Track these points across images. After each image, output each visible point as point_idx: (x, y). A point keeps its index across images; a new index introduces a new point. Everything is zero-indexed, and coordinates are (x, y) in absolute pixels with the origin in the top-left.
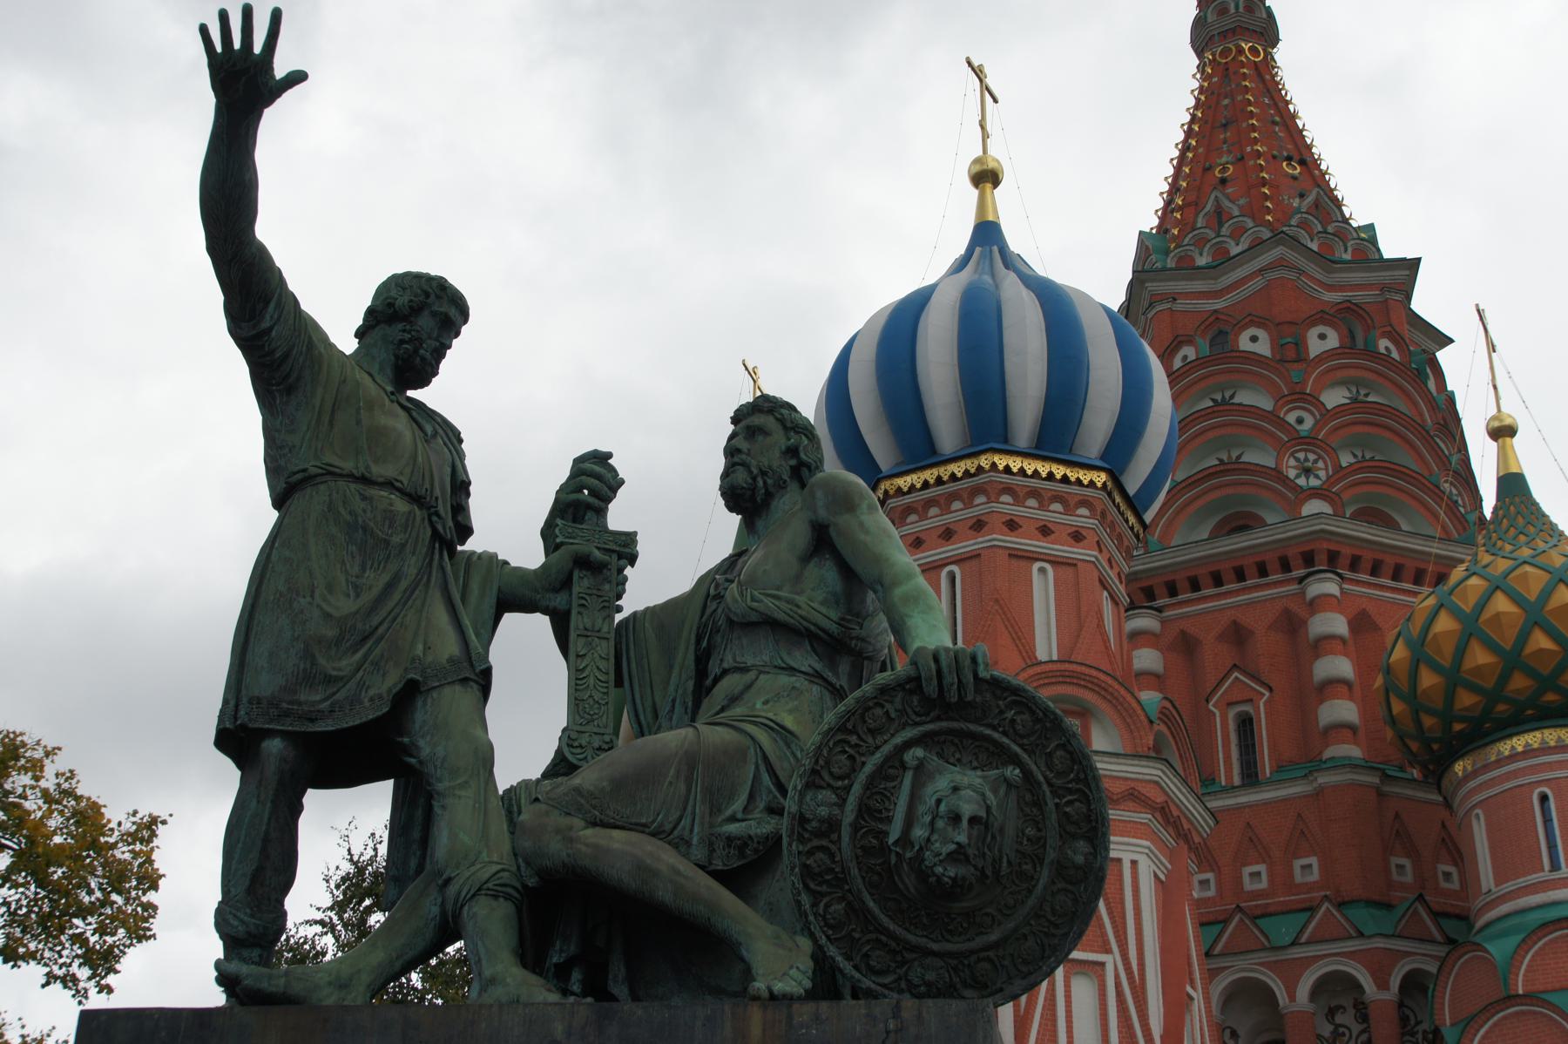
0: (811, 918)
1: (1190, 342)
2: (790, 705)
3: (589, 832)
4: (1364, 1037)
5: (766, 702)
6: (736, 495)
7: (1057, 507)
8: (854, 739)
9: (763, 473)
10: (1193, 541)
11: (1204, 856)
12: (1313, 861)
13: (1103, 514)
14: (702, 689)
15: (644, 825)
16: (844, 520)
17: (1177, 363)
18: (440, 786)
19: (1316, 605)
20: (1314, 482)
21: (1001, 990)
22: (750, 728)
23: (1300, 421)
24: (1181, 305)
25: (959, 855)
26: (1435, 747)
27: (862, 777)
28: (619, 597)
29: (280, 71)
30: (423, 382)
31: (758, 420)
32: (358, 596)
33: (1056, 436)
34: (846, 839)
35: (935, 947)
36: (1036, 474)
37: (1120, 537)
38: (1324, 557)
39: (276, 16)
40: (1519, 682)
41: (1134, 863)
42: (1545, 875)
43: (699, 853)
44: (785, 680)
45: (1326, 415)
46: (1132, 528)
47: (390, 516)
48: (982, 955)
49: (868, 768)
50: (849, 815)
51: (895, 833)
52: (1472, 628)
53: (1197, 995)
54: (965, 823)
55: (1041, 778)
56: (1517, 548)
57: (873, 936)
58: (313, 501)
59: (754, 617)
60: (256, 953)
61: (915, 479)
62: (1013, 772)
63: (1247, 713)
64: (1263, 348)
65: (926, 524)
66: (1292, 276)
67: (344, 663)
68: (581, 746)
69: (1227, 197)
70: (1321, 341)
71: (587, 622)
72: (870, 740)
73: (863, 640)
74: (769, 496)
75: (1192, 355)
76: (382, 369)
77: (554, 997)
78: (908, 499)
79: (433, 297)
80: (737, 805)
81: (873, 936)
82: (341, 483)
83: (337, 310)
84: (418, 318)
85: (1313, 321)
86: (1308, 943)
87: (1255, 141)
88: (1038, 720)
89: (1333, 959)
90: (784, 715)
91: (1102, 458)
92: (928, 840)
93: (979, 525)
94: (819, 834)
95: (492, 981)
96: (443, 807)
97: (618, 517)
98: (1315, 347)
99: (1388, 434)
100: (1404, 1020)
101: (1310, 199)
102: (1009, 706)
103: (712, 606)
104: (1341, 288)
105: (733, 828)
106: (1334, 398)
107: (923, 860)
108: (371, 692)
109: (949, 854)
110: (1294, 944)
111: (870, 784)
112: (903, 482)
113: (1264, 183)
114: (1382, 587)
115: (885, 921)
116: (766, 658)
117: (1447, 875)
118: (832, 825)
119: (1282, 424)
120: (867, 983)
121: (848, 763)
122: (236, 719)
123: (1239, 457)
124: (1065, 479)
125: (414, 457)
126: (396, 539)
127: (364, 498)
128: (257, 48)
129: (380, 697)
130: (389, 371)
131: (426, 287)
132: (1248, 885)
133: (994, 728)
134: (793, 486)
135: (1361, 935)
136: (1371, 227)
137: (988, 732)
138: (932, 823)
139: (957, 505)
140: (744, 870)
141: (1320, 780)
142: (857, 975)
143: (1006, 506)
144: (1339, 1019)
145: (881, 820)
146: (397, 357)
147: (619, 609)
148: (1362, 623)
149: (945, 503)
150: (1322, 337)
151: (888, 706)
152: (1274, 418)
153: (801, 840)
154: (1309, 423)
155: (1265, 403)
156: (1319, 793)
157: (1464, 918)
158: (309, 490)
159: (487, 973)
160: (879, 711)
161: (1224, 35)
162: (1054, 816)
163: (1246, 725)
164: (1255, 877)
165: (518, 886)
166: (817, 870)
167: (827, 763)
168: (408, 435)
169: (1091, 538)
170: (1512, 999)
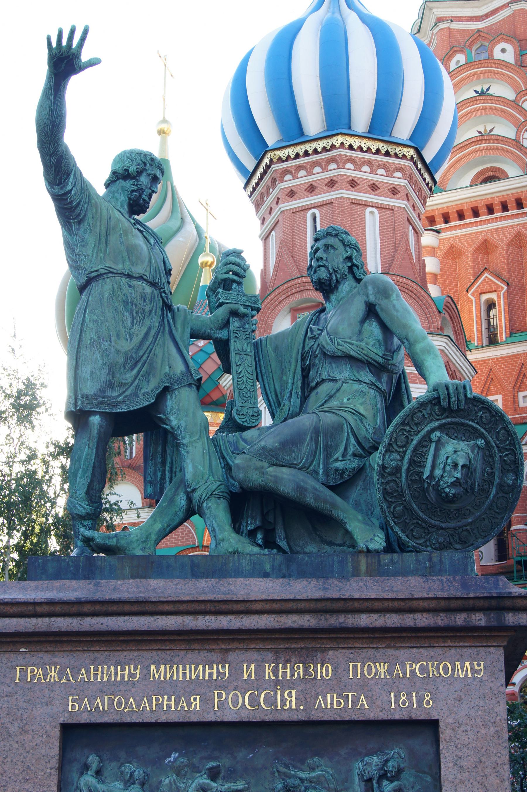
0: (387, 514)
1: (461, 51)
2: (361, 401)
3: (271, 469)
5: (348, 399)
7: (381, 171)
8: (408, 428)
9: (335, 271)
13: (411, 176)
15: (296, 464)
16: (384, 303)
17: (453, 66)
18: (185, 441)
21: (472, 544)
25: (457, 483)
31: (331, 241)
32: (131, 340)
33: (381, 124)
34: (404, 476)
35: (443, 525)
37: (420, 190)
39: (86, 32)
44: (356, 386)
46: (427, 185)
47: (143, 296)
48: (465, 528)
49: (414, 443)
50: (405, 467)
51: (426, 473)
54: (460, 467)
55: (494, 444)
57: (415, 521)
58: (104, 287)
59: (339, 354)
60: (90, 522)
61: (291, 152)
62: (481, 442)
63: (493, 300)
64: (510, 57)
67: (128, 375)
68: (243, 414)
71: (239, 346)
72: (416, 428)
73: (394, 365)
74: (338, 282)
76: (122, 206)
77: (256, 549)
78: (285, 165)
79: (148, 165)
80: (338, 454)
81: (415, 521)
82: (118, 278)
88: (493, 416)
90: (359, 406)
91: (410, 139)
92: (442, 476)
93: (332, 183)
94: (391, 474)
95: (223, 540)
96: (188, 452)
103: (310, 343)
105: (337, 465)
107: (439, 485)
108: (143, 391)
109: (452, 483)
111: (415, 450)
115: (421, 513)
116: (347, 375)
118: (397, 470)
120: (412, 543)
121: (405, 439)
123: (491, 131)
126: (147, 309)
127: (130, 286)
128: (74, 46)
129: (148, 393)
130: (126, 207)
131: (144, 160)
133: (473, 421)
134: (350, 277)
137: (470, 423)
138: (444, 468)
139: (317, 169)
140: (342, 485)
142: (408, 540)
145: (420, 467)
146: (130, 199)
149: (309, 169)
151: (424, 412)
153: (383, 477)
155: (510, 95)
158: (100, 282)
159: (220, 536)
160: (420, 414)
162: (499, 462)
165: (228, 491)
166: (390, 491)
167: (396, 440)
168: (145, 247)
169: (402, 193)
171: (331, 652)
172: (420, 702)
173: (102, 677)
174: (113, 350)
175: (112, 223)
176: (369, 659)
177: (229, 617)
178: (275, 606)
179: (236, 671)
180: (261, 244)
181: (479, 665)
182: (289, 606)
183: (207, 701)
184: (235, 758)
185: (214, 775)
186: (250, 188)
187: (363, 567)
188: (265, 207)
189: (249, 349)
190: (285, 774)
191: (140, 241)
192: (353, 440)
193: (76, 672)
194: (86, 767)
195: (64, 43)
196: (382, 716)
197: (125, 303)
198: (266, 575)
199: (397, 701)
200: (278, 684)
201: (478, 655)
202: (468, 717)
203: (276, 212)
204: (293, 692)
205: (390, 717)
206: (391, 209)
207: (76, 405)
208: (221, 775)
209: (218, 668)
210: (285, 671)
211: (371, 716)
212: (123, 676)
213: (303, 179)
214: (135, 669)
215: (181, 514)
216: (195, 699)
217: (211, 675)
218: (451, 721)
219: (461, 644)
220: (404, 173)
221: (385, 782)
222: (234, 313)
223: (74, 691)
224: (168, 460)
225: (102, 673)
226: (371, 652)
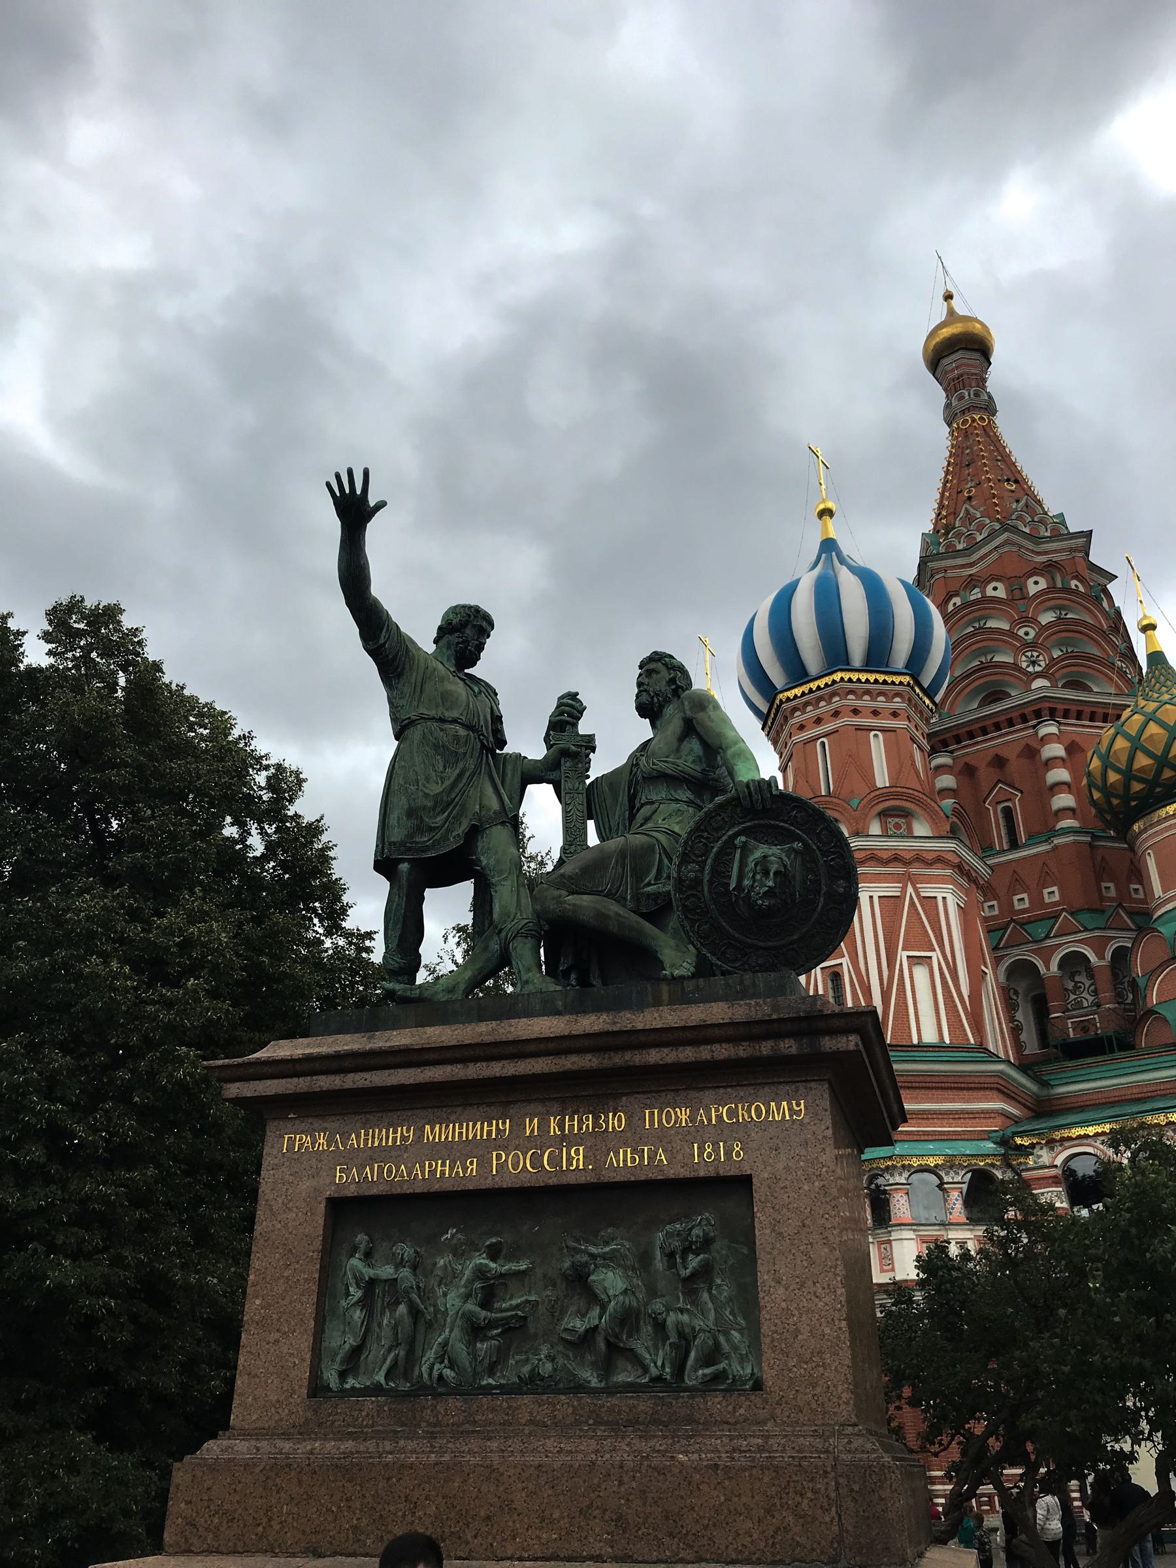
1: (957, 595)
4: (1092, 988)
6: (644, 710)
8: (705, 834)
9: (657, 695)
10: (970, 710)
11: (988, 890)
12: (1055, 889)
14: (632, 817)
15: (602, 891)
17: (950, 608)
19: (1045, 740)
20: (1038, 669)
22: (654, 834)
23: (1027, 634)
24: (950, 574)
25: (770, 893)
28: (588, 770)
29: (372, 503)
30: (473, 664)
31: (652, 666)
35: (762, 944)
36: (867, 681)
37: (921, 712)
38: (1047, 712)
39: (366, 473)
41: (944, 898)
43: (629, 904)
44: (674, 806)
47: (457, 738)
49: (715, 850)
50: (706, 878)
51: (733, 885)
53: (989, 971)
56: (1161, 694)
58: (415, 734)
59: (655, 774)
60: (406, 978)
61: (797, 691)
62: (798, 845)
66: (1015, 549)
70: (1035, 586)
73: (716, 780)
74: (661, 707)
75: (959, 603)
76: (449, 660)
78: (793, 703)
80: (651, 877)
83: (421, 628)
84: (467, 630)
86: (1055, 937)
87: (987, 472)
89: (1071, 945)
91: (906, 667)
93: (836, 714)
95: (527, 982)
97: (584, 728)
98: (1032, 589)
99: (1079, 636)
100: (1115, 975)
101: (1023, 502)
102: (793, 808)
103: (635, 770)
104: (1046, 553)
106: (1046, 618)
110: (1047, 937)
111: (717, 858)
112: (791, 694)
113: (994, 496)
114: (1084, 726)
117: (1136, 890)
118: (697, 882)
122: (383, 854)
125: (468, 705)
126: (461, 750)
127: (442, 730)
128: (359, 492)
132: (1017, 906)
135: (1086, 930)
138: (754, 876)
139: (823, 703)
141: (1055, 842)
144: (1077, 979)
145: (725, 877)
147: (588, 777)
148: (1073, 748)
150: (1036, 583)
152: (1011, 634)
153: (681, 892)
154: (1032, 634)
155: (1005, 626)
156: (1056, 848)
157: (1148, 914)
159: (524, 978)
160: (719, 818)
161: (963, 412)
163: (1008, 814)
164: (1021, 901)
168: (464, 693)
169: (903, 715)
171: (624, 1099)
172: (728, 1153)
173: (373, 1142)
174: (421, 794)
175: (429, 671)
176: (668, 1105)
177: (503, 1062)
178: (551, 1046)
179: (518, 1126)
181: (798, 1105)
183: (484, 1164)
185: (494, 1253)
186: (767, 729)
187: (665, 997)
190: (574, 1248)
193: (345, 1137)
194: (355, 1249)
196: (684, 1173)
198: (558, 1013)
199: (700, 1155)
200: (567, 1140)
201: (796, 1092)
202: (787, 1168)
204: (581, 1149)
208: (504, 1252)
209: (497, 1125)
210: (572, 1124)
211: (671, 1174)
212: (395, 1139)
214: (408, 1131)
216: (472, 1163)
217: (489, 1133)
218: (766, 1175)
219: (776, 1080)
221: (691, 1257)
223: (342, 1160)
225: (373, 1138)
226: (670, 1096)
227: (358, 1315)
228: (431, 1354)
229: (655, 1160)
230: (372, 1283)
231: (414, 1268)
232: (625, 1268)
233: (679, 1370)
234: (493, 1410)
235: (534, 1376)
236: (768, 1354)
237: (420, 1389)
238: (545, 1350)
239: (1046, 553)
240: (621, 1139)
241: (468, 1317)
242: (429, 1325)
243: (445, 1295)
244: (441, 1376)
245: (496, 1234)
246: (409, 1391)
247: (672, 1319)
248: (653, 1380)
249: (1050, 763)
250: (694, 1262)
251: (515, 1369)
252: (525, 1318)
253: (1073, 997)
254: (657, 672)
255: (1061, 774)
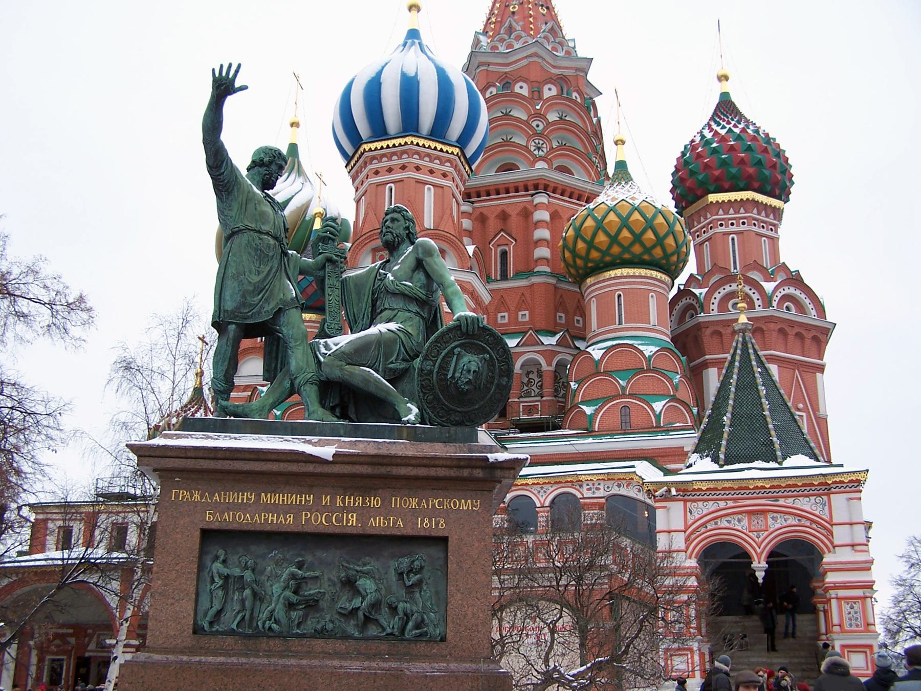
7: (437, 161)
12: (527, 313)
16: (428, 259)
19: (537, 207)
20: (541, 153)
23: (538, 126)
24: (491, 68)
25: (469, 382)
26: (581, 272)
27: (441, 357)
31: (395, 215)
33: (439, 131)
36: (429, 147)
40: (616, 250)
42: (616, 326)
44: (407, 314)
45: (549, 124)
47: (269, 246)
49: (443, 354)
52: (600, 225)
59: (397, 292)
61: (378, 145)
65: (381, 165)
69: (515, 21)
70: (550, 91)
74: (399, 244)
80: (393, 358)
83: (241, 159)
85: (547, 82)
91: (457, 142)
93: (403, 168)
94: (426, 375)
98: (547, 94)
100: (556, 377)
101: (549, 25)
103: (378, 283)
104: (559, 68)
105: (392, 366)
106: (552, 117)
113: (531, 16)
114: (564, 201)
117: (578, 321)
118: (431, 372)
119: (530, 127)
124: (441, 150)
126: (271, 254)
128: (230, 76)
132: (500, 321)
134: (407, 241)
136: (574, 40)
139: (395, 157)
143: (416, 160)
144: (531, 376)
148: (555, 215)
150: (550, 89)
152: (527, 123)
153: (421, 376)
155: (525, 117)
163: (504, 254)
169: (450, 177)
170: (598, 373)
171: (380, 491)
172: (437, 524)
179: (318, 499)
180: (354, 204)
182: (354, 459)
183: (297, 517)
184: (314, 556)
186: (349, 167)
188: (358, 181)
189: (338, 284)
191: (268, 209)
192: (403, 349)
193: (212, 495)
194: (216, 558)
195: (224, 74)
197: (256, 250)
203: (366, 184)
205: (417, 534)
206: (442, 187)
207: (219, 317)
212: (243, 499)
213: (385, 163)
215: (287, 392)
217: (301, 501)
220: (452, 164)
221: (411, 575)
222: (329, 260)
224: (280, 355)
227: (220, 593)
228: (264, 615)
229: (398, 525)
230: (227, 578)
231: (253, 570)
232: (374, 578)
233: (403, 630)
234: (302, 645)
235: (324, 629)
236: (450, 625)
237: (257, 635)
238: (328, 617)
239: (559, 68)
240: (377, 512)
241: (287, 599)
242: (262, 600)
243: (271, 586)
244: (270, 628)
245: (301, 556)
246: (251, 633)
247: (401, 606)
248: (387, 634)
249: (538, 224)
250: (414, 578)
251: (311, 625)
252: (318, 601)
253: (526, 388)
254: (398, 221)
255: (543, 233)
